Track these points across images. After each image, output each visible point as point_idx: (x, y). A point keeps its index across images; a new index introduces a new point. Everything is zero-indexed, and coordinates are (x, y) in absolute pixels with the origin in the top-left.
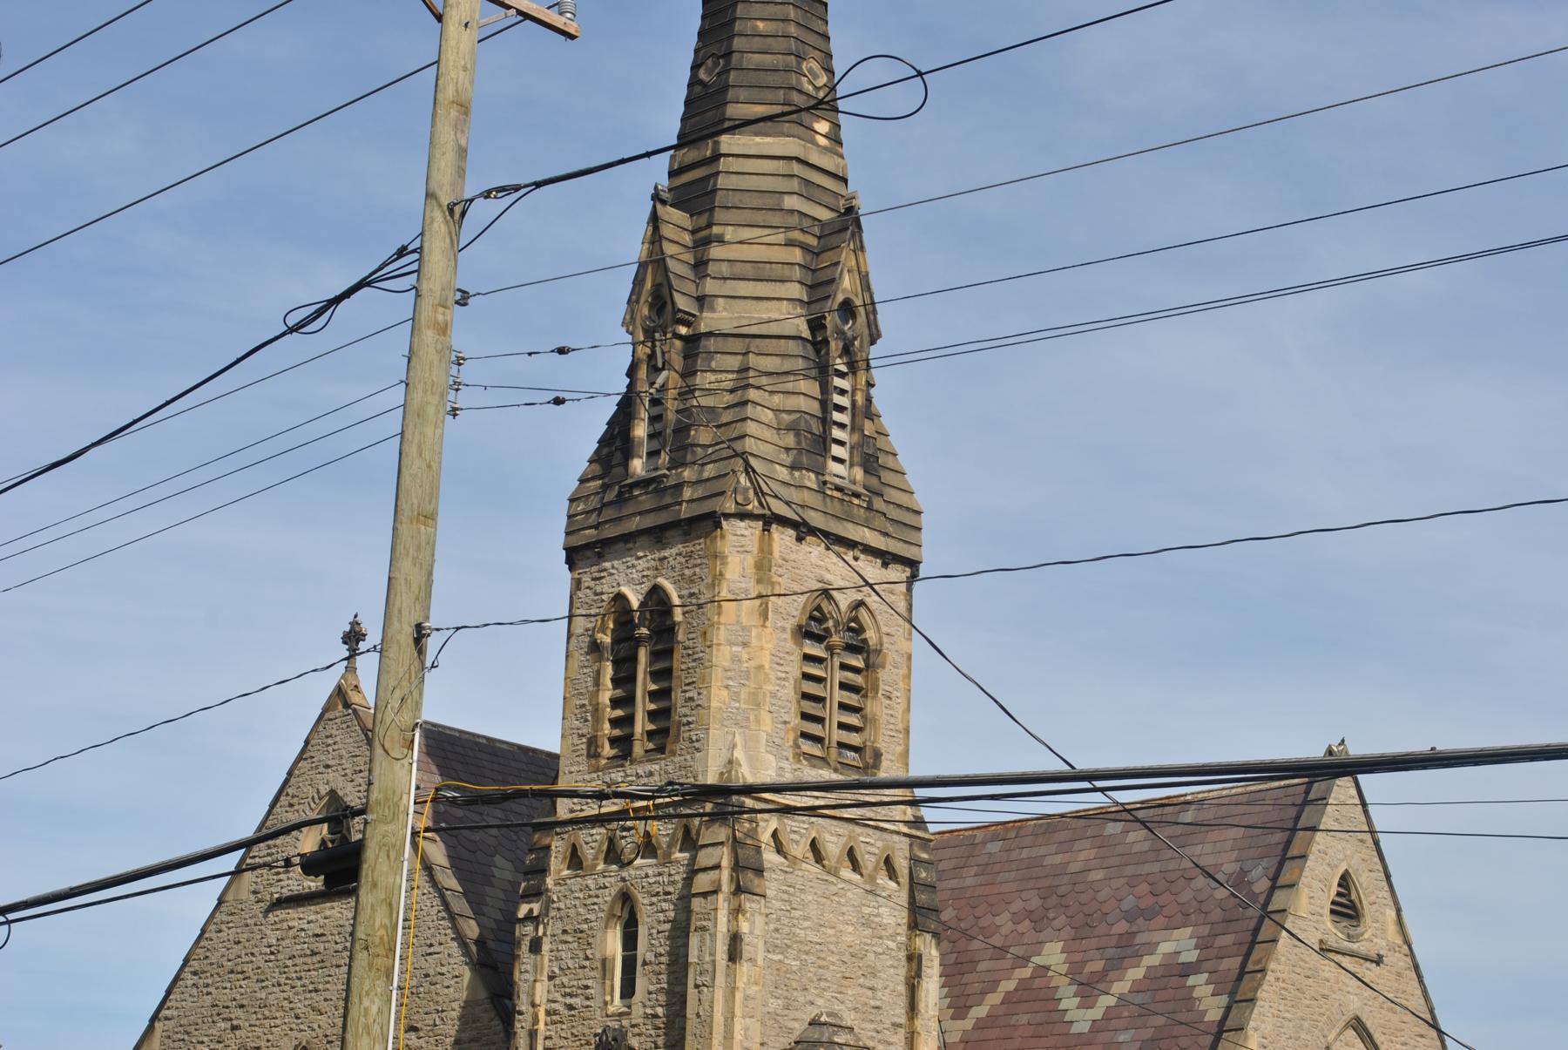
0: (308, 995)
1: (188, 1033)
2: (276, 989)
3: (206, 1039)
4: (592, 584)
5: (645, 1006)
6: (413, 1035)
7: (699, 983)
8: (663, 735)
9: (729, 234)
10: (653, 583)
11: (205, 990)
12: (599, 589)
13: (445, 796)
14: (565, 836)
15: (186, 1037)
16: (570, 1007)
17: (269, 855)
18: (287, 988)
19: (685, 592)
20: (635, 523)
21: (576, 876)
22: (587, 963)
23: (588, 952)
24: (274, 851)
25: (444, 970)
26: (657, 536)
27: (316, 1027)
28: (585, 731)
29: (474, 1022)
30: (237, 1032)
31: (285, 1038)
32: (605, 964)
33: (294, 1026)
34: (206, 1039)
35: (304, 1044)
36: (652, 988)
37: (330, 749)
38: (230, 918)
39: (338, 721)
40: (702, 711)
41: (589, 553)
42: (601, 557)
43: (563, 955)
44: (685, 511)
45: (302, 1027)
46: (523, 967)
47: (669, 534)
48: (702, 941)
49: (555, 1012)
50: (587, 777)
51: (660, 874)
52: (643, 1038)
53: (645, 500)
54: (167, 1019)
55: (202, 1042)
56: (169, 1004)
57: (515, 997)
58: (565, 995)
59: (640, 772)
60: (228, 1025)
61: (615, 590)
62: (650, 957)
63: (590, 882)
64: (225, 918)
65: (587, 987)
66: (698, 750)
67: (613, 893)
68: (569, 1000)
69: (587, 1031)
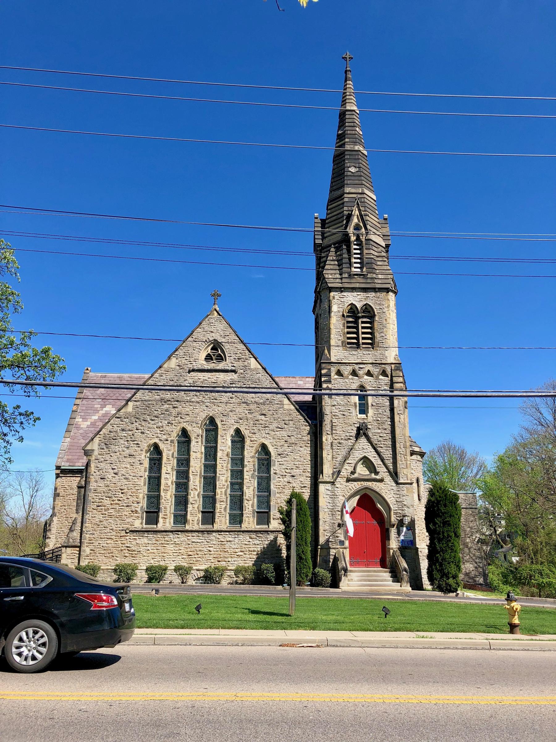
0: (212, 401)
1: (148, 407)
2: (196, 397)
3: (159, 410)
4: (339, 299)
5: (373, 417)
6: (263, 417)
7: (399, 412)
8: (373, 344)
9: (370, 215)
10: (365, 303)
11: (156, 394)
12: (342, 301)
13: (324, 350)
14: (336, 367)
15: (147, 408)
16: (344, 415)
17: (185, 355)
18: (201, 397)
19: (378, 307)
20: (357, 285)
21: (341, 378)
22: (348, 403)
23: (349, 400)
24: (188, 354)
25: (274, 399)
26: (365, 290)
27: (216, 410)
28: (340, 339)
29: (290, 415)
30: (176, 409)
31: (201, 413)
32: (355, 403)
33: (205, 409)
34: (159, 410)
35: (211, 415)
36: (375, 413)
37: (212, 327)
38: (167, 373)
39: (215, 319)
40: (387, 340)
41: (338, 290)
42: (342, 292)
43: (338, 400)
44: (378, 286)
45: (209, 410)
46: (326, 402)
47: (369, 290)
48: (399, 402)
49: (337, 416)
50: (343, 352)
51: (375, 382)
52: (373, 426)
53: (362, 280)
54: (135, 401)
55: (158, 411)
56: (135, 397)
57: (324, 410)
58: (340, 411)
59: (364, 353)
60: (171, 406)
61: (350, 302)
62: (374, 404)
63: (347, 380)
64: (163, 372)
65: (349, 410)
66: (386, 350)
67: (357, 385)
68: (342, 413)
69: (351, 422)
